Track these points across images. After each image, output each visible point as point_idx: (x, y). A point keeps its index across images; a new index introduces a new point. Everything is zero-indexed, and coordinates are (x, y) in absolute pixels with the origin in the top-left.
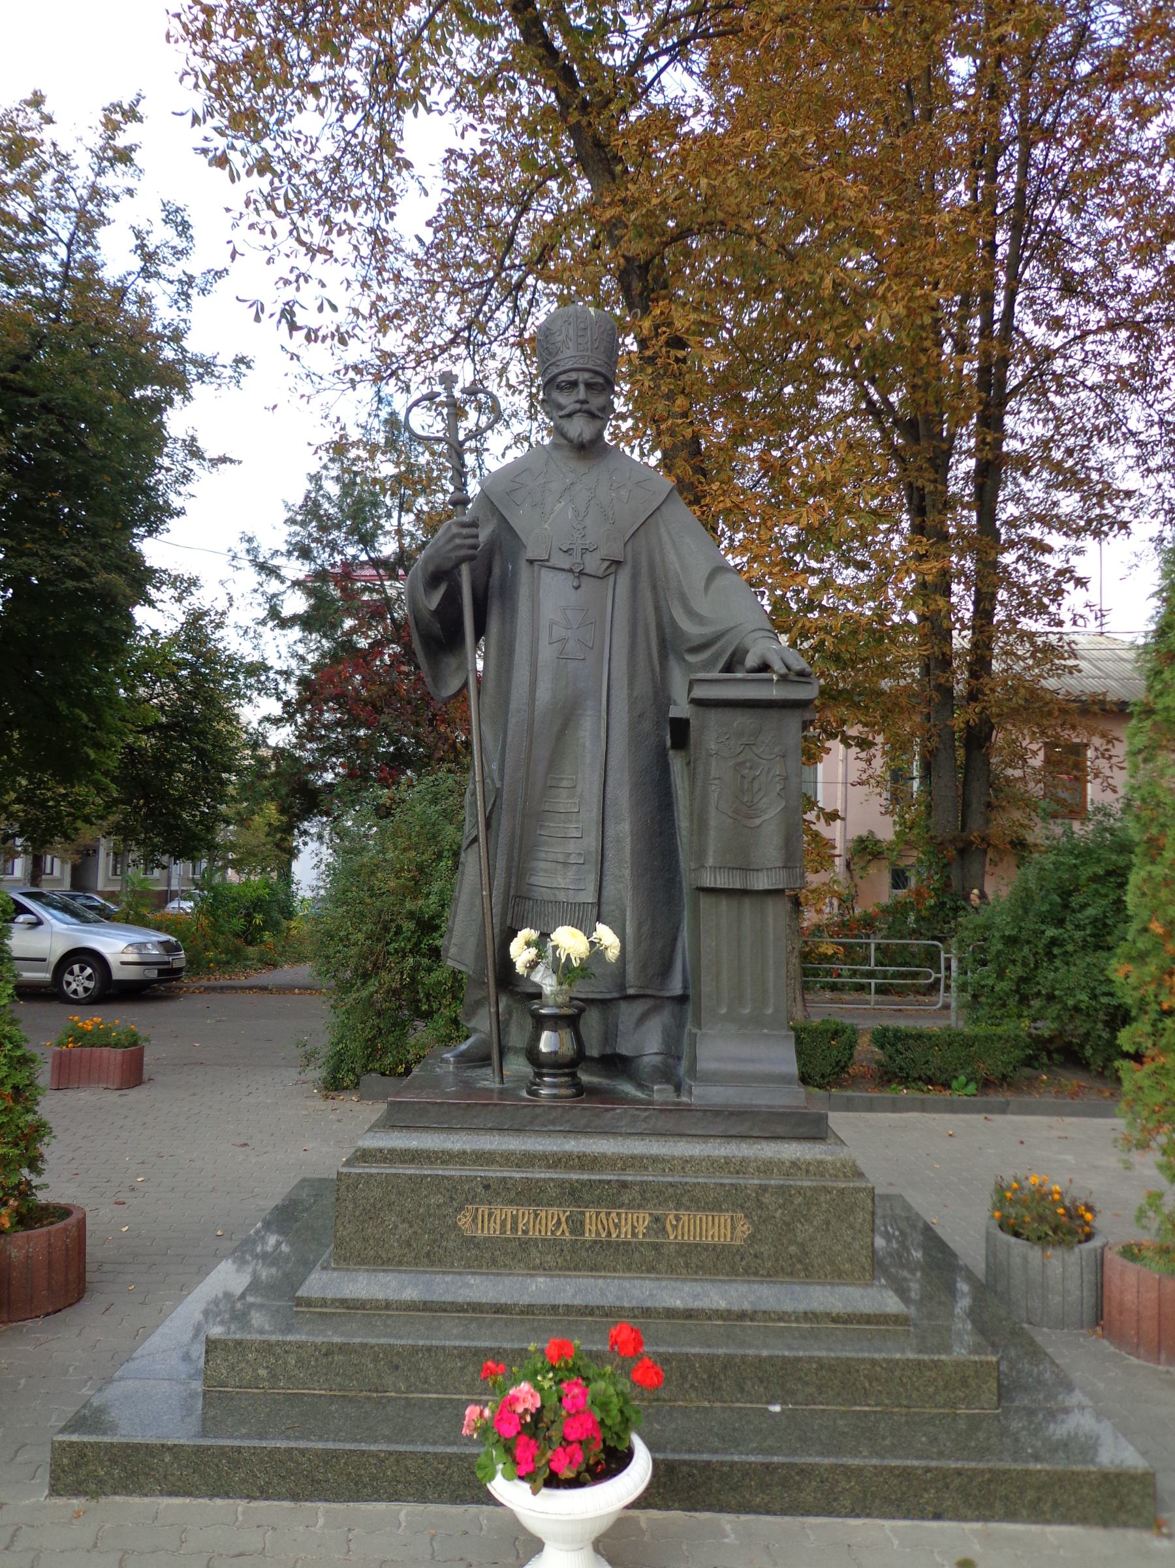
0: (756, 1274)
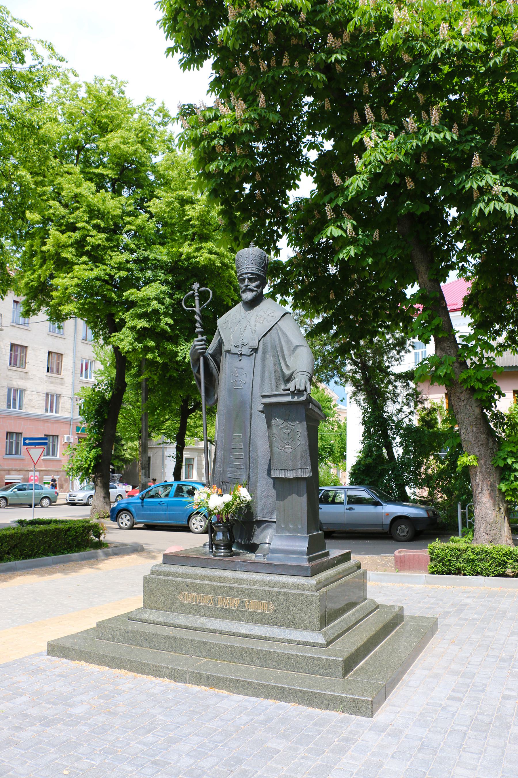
0: (276, 625)
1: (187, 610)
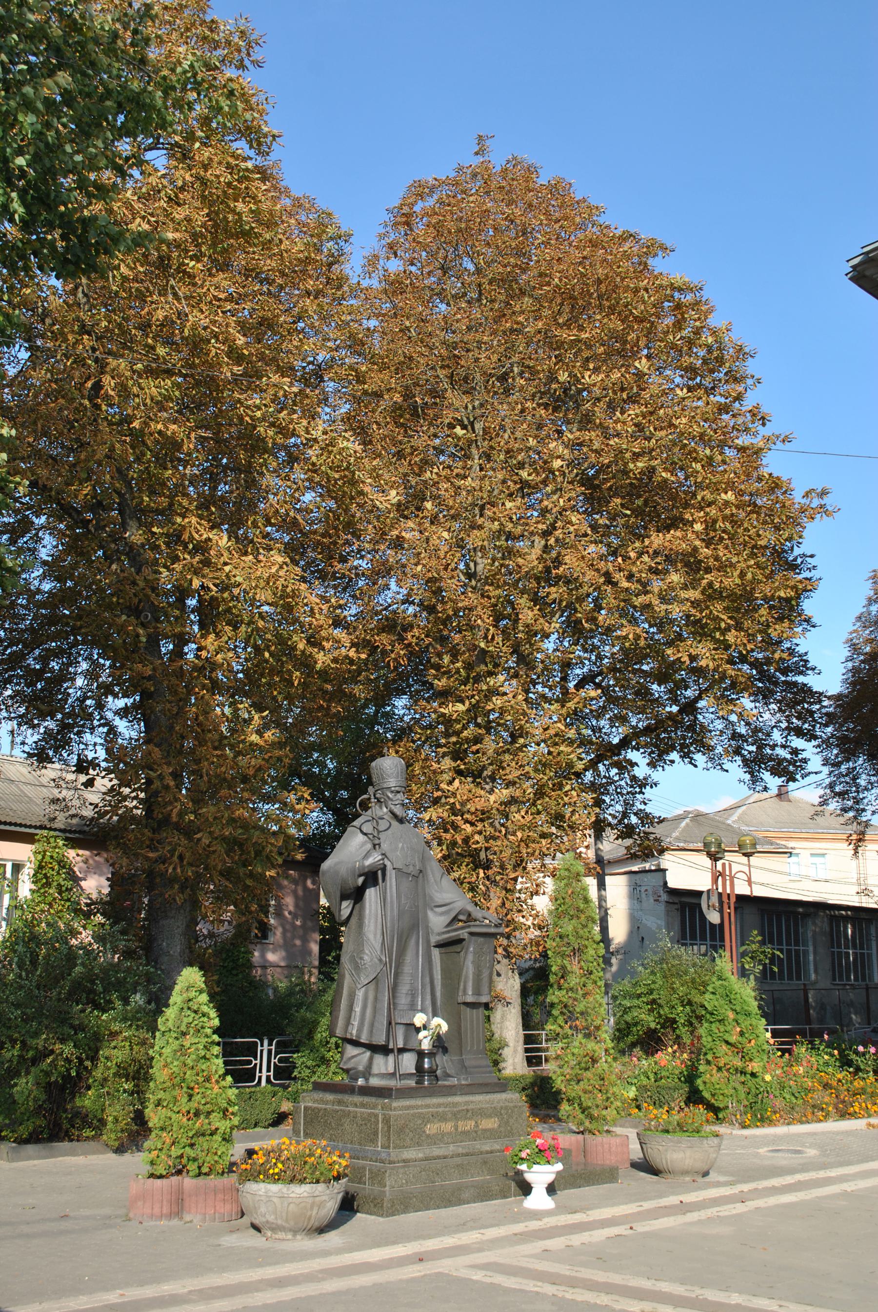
1: (434, 1140)
